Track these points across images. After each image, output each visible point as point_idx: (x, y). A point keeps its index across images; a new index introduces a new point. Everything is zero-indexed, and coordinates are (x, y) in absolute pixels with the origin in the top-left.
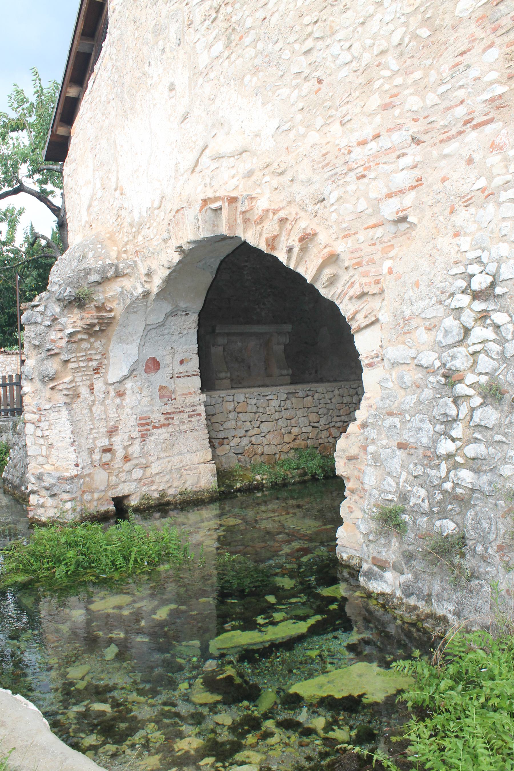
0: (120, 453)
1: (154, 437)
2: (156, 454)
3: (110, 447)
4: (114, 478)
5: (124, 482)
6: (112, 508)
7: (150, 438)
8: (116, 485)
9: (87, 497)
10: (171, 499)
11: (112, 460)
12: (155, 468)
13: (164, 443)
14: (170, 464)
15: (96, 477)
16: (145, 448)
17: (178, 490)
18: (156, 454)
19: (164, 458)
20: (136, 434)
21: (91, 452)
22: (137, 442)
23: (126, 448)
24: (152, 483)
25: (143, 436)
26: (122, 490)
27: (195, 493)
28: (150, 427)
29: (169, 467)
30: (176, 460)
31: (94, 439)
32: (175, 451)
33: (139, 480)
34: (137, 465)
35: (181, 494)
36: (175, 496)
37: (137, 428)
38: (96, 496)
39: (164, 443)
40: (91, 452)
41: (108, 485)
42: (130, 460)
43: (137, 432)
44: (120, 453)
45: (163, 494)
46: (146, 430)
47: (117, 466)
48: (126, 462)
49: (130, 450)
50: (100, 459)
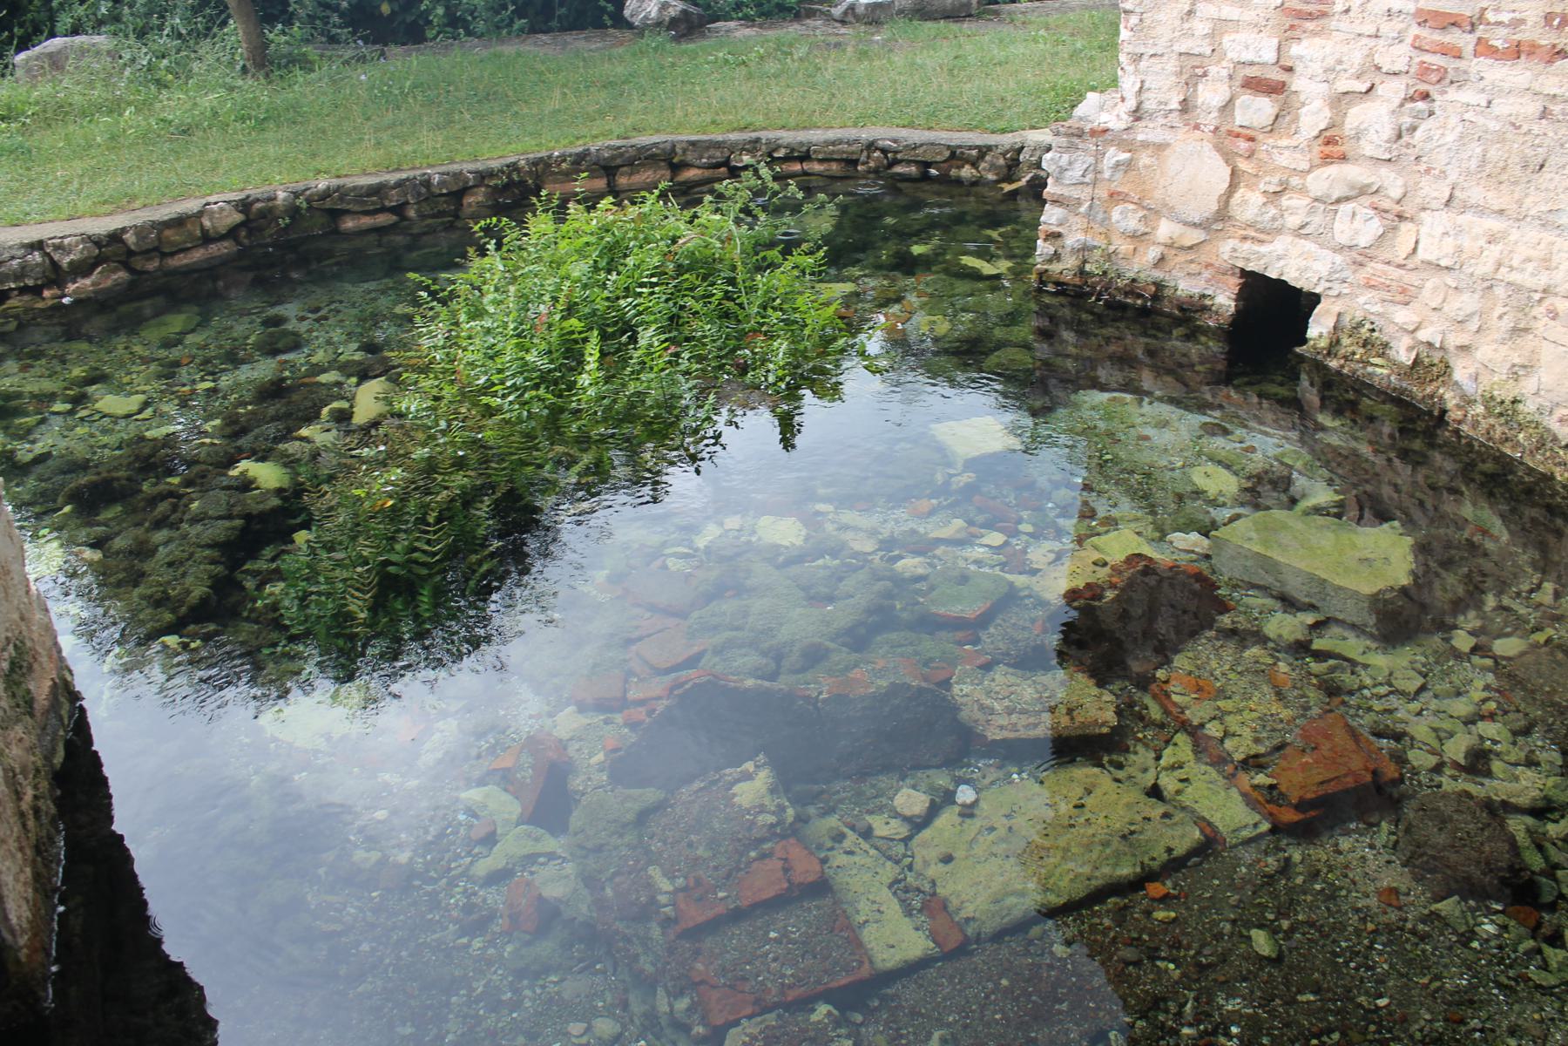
0: (1313, 118)
1: (1467, 96)
2: (1453, 177)
3: (1276, 75)
4: (1256, 199)
5: (1300, 232)
6: (1225, 300)
7: (1452, 94)
8: (1264, 233)
9: (1125, 218)
10: (1451, 399)
11: (1272, 129)
12: (1433, 235)
13: (1501, 139)
14: (1494, 251)
15: (1173, 162)
16: (1418, 134)
17: (1486, 382)
18: (1453, 177)
19: (1481, 210)
20: (1397, 56)
21: (1193, 73)
22: (1392, 91)
23: (1341, 101)
24: (1406, 296)
25: (1424, 71)
26: (1292, 263)
27: (1545, 441)
28: (1465, 41)
29: (1484, 267)
30: (1527, 240)
31: (1221, 26)
32: (1535, 204)
33: (1361, 257)
34: (1363, 191)
35: (1489, 400)
36: (1468, 401)
37: (1415, 30)
38: (1165, 230)
39: (1501, 139)
40: (1193, 73)
41: (1223, 215)
42: (1343, 158)
43: (1404, 49)
44: (1313, 118)
45: (1431, 366)
46: (1445, 50)
47: (1284, 160)
48: (1327, 159)
49: (1356, 116)
50: (1227, 107)
